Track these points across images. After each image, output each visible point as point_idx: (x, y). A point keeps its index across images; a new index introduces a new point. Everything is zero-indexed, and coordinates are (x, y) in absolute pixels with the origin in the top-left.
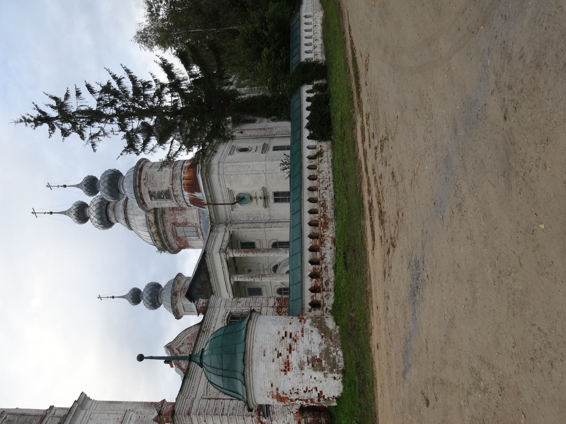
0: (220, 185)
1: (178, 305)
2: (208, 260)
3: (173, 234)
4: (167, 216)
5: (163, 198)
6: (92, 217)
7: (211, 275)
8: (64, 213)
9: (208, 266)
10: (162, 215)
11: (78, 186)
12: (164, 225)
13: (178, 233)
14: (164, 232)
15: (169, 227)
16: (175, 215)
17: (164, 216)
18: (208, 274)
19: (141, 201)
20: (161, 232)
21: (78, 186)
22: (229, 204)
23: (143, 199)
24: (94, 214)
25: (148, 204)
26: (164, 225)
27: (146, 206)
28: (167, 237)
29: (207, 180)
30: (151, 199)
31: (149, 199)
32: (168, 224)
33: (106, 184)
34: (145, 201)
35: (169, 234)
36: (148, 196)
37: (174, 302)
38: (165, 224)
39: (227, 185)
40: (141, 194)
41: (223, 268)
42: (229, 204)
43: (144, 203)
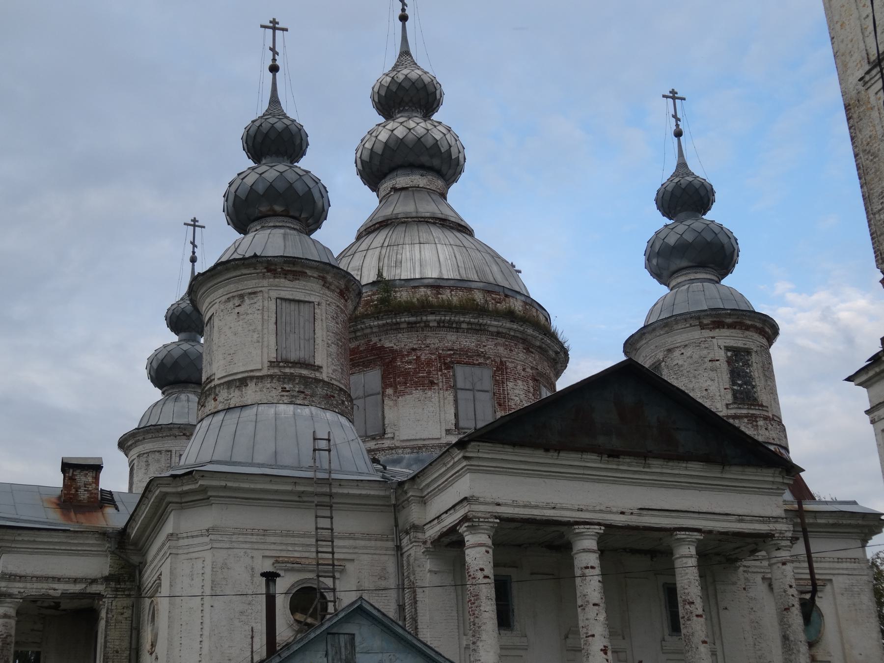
0: (840, 560)
1: (316, 286)
2: (768, 476)
3: (464, 352)
4: (522, 356)
5: (734, 383)
6: (391, 125)
7: (714, 472)
8: (405, 53)
9: (749, 470)
10: (524, 341)
11: (682, 165)
12: (499, 334)
13: (468, 369)
14: (479, 330)
15: (492, 348)
16: (524, 379)
17: (521, 346)
18: (723, 462)
19: (729, 320)
20: (486, 321)
21: (682, 165)
22: (812, 573)
23: (731, 326)
24: (400, 132)
25: (707, 333)
26: (499, 334)
27: (703, 327)
28: (458, 329)
29: (850, 525)
30: (727, 349)
31: (732, 343)
32: (501, 349)
33: (689, 237)
34: (726, 332)
35: (468, 342)
36: (740, 344)
37: (329, 278)
38: (501, 340)
39: (841, 578)
40: (748, 328)
41: (741, 518)
42: (812, 573)
43: (718, 324)
